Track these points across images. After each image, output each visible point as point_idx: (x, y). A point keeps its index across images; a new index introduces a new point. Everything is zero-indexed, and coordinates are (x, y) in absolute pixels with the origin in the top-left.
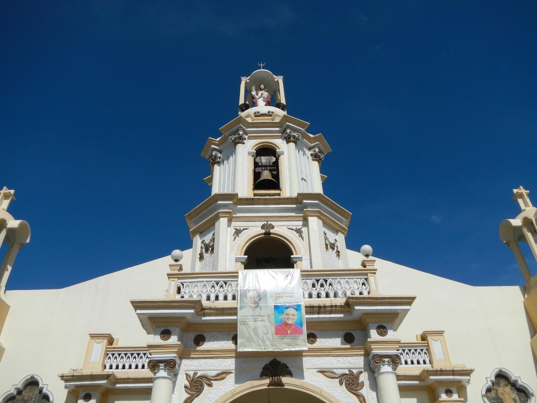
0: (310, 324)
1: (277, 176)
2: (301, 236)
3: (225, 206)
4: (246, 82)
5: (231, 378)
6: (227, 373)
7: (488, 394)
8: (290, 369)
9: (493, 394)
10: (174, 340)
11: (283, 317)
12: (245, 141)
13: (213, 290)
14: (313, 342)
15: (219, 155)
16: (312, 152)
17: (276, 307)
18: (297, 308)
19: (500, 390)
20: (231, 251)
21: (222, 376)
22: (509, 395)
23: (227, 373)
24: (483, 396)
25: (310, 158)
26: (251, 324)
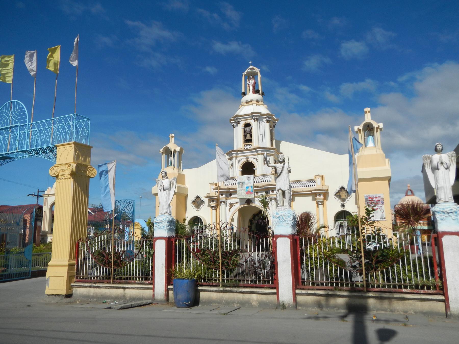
0: (254, 190)
1: (251, 136)
2: (257, 161)
3: (234, 154)
4: (245, 75)
5: (239, 204)
6: (238, 202)
7: (337, 194)
8: (252, 201)
9: (338, 194)
10: (224, 196)
11: (248, 190)
12: (241, 122)
13: (232, 182)
14: (257, 194)
15: (235, 124)
16: (266, 119)
17: (246, 187)
18: (252, 187)
19: (341, 193)
20: (238, 167)
21: (236, 203)
22: (344, 194)
23: (238, 202)
24: (334, 195)
25: (265, 122)
26: (240, 192)
